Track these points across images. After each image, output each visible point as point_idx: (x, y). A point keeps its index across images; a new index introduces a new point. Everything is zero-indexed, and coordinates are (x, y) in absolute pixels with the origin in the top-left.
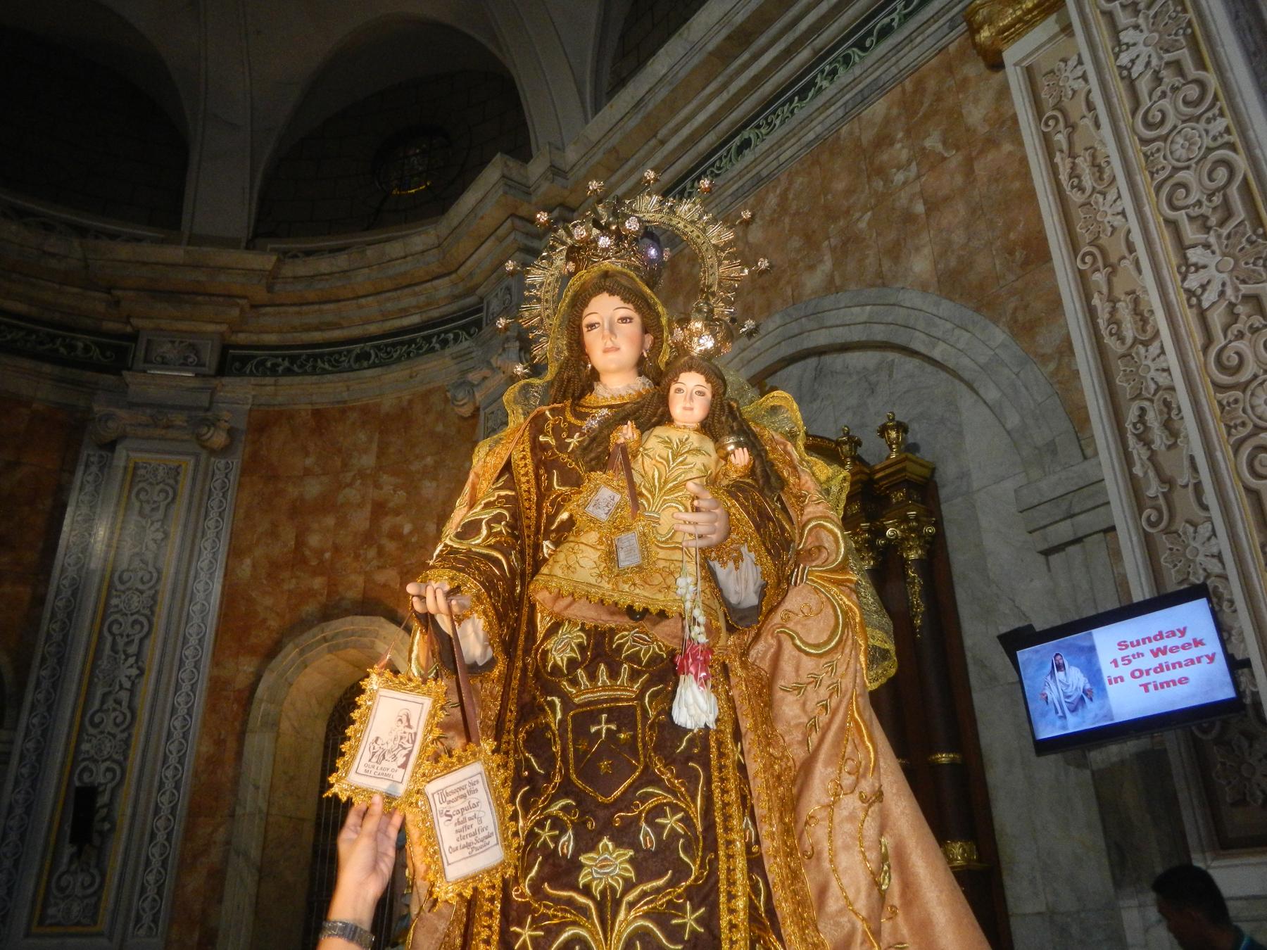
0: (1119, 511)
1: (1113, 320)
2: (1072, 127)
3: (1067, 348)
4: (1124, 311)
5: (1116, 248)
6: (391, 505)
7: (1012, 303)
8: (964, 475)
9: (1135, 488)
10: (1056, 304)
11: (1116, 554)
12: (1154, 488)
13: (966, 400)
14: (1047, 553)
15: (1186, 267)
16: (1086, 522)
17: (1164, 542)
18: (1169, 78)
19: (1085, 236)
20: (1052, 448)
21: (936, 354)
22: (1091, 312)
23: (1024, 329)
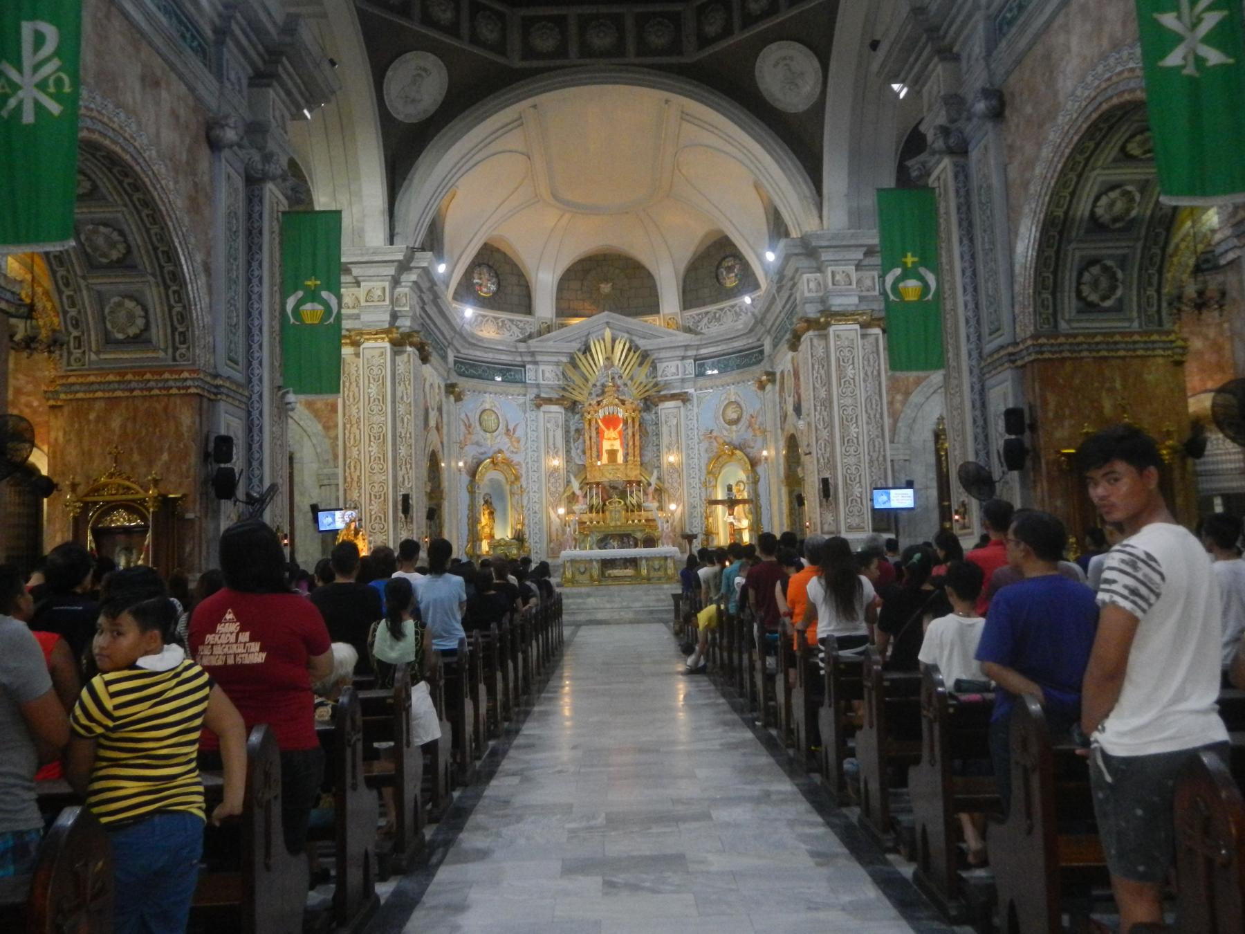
0: (341, 481)
1: (349, 438)
2: (351, 383)
3: (336, 438)
4: (352, 436)
5: (354, 421)
6: (25, 390)
7: (324, 420)
8: (302, 458)
9: (345, 479)
10: (336, 426)
11: (338, 490)
12: (349, 479)
13: (306, 438)
14: (321, 486)
15: (370, 446)
16: (332, 482)
17: (348, 492)
18: (377, 402)
19: (347, 414)
20: (327, 461)
21: (301, 423)
22: (345, 434)
23: (327, 428)
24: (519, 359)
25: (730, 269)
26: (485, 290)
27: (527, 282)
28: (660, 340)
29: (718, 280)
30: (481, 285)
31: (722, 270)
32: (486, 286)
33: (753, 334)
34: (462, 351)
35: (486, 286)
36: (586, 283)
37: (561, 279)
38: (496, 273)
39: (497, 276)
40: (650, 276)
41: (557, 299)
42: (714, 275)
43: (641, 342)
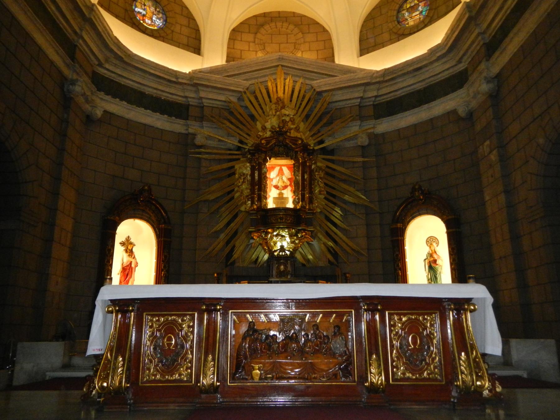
24: (182, 94)
25: (413, 9)
26: (149, 22)
27: (197, 26)
28: (337, 79)
29: (399, 22)
30: (144, 15)
31: (404, 12)
32: (151, 19)
33: (451, 55)
34: (107, 66)
35: (151, 19)
36: (259, 36)
37: (234, 30)
38: (163, 10)
39: (164, 12)
40: (325, 30)
41: (228, 48)
42: (395, 18)
43: (315, 83)
